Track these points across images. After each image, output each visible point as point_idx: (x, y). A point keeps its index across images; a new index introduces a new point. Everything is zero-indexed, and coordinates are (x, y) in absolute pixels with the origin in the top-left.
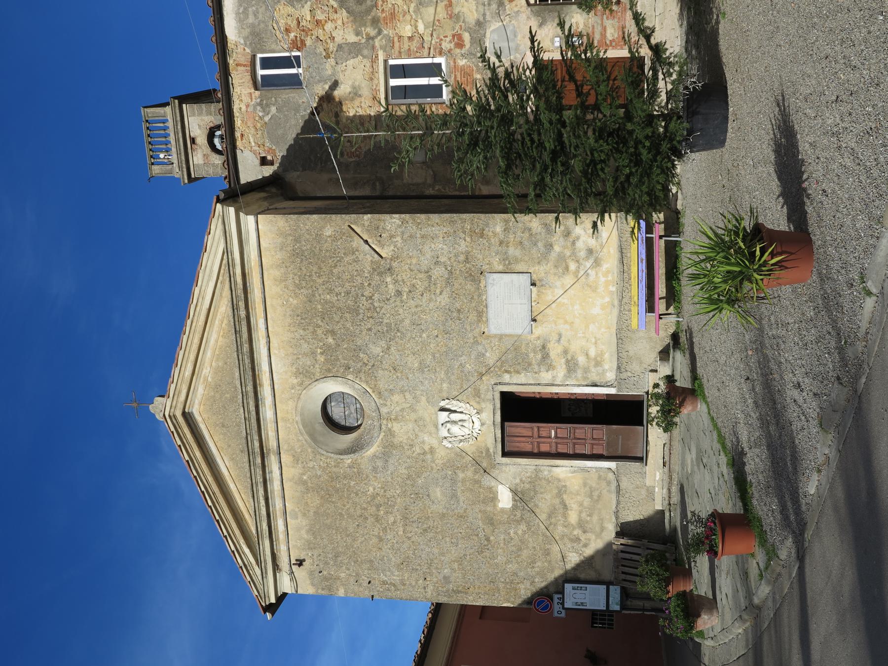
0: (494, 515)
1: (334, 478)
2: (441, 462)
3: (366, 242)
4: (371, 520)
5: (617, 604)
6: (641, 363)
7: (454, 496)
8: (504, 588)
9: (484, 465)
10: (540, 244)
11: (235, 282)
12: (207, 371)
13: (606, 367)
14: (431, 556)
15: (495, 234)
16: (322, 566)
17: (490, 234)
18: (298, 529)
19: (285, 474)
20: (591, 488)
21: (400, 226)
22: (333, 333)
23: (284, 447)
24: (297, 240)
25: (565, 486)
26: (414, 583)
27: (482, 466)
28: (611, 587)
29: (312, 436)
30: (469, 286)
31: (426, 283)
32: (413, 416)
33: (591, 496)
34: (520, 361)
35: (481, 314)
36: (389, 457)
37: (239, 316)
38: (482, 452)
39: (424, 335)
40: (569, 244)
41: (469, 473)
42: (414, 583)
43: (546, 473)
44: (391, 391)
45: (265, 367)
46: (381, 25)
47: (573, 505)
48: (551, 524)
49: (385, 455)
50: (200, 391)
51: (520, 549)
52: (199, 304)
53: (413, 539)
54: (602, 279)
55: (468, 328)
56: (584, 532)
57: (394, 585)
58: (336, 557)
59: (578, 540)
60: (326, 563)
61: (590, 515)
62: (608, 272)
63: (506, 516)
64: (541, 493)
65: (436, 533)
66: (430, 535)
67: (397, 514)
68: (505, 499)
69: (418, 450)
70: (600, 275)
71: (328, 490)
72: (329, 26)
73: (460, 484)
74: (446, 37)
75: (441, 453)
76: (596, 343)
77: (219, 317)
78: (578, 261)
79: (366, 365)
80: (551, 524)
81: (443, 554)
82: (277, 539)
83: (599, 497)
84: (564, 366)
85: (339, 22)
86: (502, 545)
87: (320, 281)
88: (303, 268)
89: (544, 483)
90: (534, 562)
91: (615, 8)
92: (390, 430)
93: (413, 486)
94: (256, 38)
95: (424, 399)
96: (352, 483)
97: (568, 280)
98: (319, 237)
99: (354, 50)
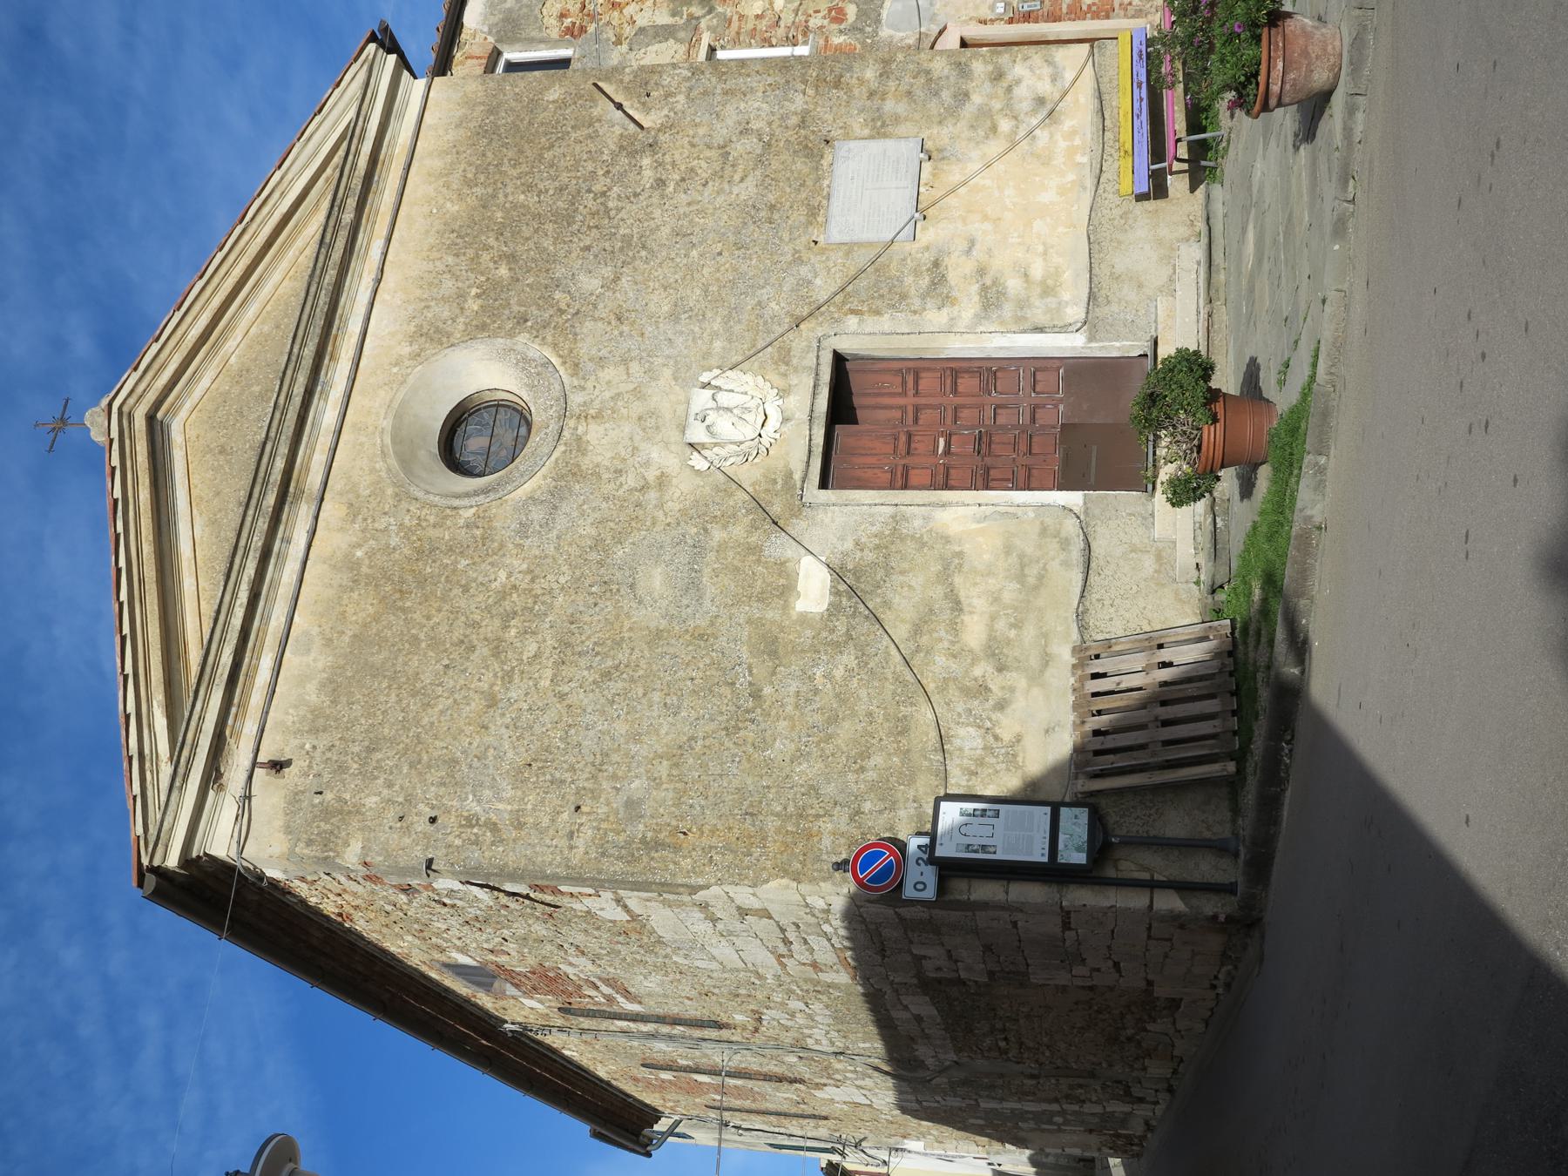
1: (424, 552)
2: (677, 507)
3: (619, 107)
4: (483, 651)
5: (1079, 849)
6: (1140, 286)
7: (693, 586)
8: (778, 831)
9: (776, 509)
10: (946, 95)
12: (234, 346)
14: (607, 743)
15: (861, 81)
16: (326, 777)
17: (854, 81)
18: (302, 680)
20: (1021, 556)
22: (512, 258)
24: (492, 111)
25: (960, 555)
26: (546, 821)
28: (1064, 811)
30: (801, 165)
31: (717, 166)
32: (637, 408)
33: (1021, 577)
34: (884, 291)
35: (815, 212)
36: (562, 499)
37: (338, 221)
38: (775, 482)
39: (694, 253)
40: (1000, 92)
41: (738, 531)
42: (546, 821)
43: (917, 523)
44: (601, 362)
45: (354, 327)
48: (918, 649)
49: (555, 497)
50: (206, 381)
51: (834, 720)
54: (1062, 145)
55: (786, 236)
57: (494, 827)
58: (370, 750)
59: (983, 689)
60: (342, 769)
61: (1016, 625)
63: (809, 633)
64: (902, 573)
65: (632, 680)
66: (616, 686)
68: (813, 590)
69: (631, 481)
70: (1058, 137)
71: (402, 579)
73: (711, 556)
74: (817, 12)
75: (682, 488)
76: (1045, 253)
77: (299, 243)
78: (1015, 118)
79: (562, 312)
80: (918, 649)
81: (636, 737)
82: (243, 706)
83: (1041, 578)
84: (976, 298)
86: (789, 708)
87: (514, 173)
88: (489, 154)
90: (865, 755)
92: (579, 439)
93: (601, 564)
95: (667, 373)
96: (464, 562)
97: (994, 147)
98: (534, 105)
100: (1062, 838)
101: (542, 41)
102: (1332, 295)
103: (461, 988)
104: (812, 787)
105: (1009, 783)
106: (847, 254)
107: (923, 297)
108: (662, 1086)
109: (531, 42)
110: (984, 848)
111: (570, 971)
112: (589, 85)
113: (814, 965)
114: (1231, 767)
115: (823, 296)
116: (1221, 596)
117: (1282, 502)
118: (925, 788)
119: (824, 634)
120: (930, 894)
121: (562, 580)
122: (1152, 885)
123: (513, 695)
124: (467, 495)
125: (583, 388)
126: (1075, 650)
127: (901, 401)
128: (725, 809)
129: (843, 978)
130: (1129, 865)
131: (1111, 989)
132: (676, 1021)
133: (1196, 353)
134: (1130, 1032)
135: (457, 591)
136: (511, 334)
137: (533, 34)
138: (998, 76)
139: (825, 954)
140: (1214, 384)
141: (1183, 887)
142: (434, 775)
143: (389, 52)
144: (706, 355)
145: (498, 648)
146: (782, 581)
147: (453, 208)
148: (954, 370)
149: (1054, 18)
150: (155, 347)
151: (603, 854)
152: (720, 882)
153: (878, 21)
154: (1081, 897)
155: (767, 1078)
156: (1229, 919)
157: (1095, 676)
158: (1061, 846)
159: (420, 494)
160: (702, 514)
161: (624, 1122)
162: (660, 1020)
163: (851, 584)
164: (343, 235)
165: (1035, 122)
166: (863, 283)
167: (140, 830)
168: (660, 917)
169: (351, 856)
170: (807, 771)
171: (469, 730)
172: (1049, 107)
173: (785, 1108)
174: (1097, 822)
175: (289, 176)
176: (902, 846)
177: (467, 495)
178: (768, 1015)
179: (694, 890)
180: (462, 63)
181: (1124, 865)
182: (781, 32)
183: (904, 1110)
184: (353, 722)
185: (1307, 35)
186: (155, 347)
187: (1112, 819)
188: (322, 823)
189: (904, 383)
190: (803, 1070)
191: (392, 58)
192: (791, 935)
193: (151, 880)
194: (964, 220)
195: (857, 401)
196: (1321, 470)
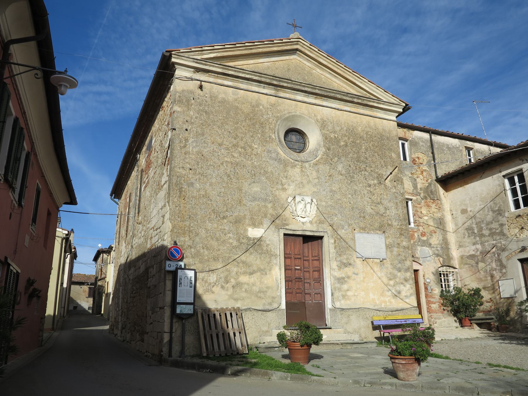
0: (243, 224)
3: (391, 173)
4: (235, 142)
5: (181, 311)
6: (346, 323)
7: (254, 199)
8: (185, 225)
9: (277, 221)
10: (400, 265)
11: (370, 101)
12: (318, 71)
13: (342, 302)
15: (402, 241)
16: (198, 101)
18: (225, 93)
19: (262, 97)
20: (266, 291)
21: (400, 192)
22: (346, 145)
24: (388, 138)
25: (266, 274)
26: (187, 161)
27: (276, 220)
28: (192, 306)
29: (287, 119)
30: (377, 225)
31: (375, 201)
32: (305, 182)
33: (260, 292)
35: (363, 229)
37: (354, 98)
38: (285, 221)
39: (350, 196)
40: (401, 281)
42: (187, 161)
43: (275, 261)
44: (318, 171)
45: (325, 103)
46: (425, 200)
47: (253, 279)
48: (238, 263)
49: (279, 160)
50: (308, 64)
51: (217, 240)
52: (359, 79)
53: (221, 167)
54: (387, 299)
55: (356, 221)
56: (233, 287)
57: (185, 147)
58: (206, 112)
60: (201, 105)
62: (391, 303)
63: (242, 232)
64: (260, 258)
65: (227, 183)
66: (226, 179)
67: (240, 159)
68: (254, 233)
69: (284, 181)
70: (389, 298)
71: (254, 119)
72: (421, 176)
73: (263, 204)
75: (283, 195)
77: (348, 88)
79: (331, 160)
80: (238, 263)
81: (211, 185)
82: (217, 77)
83: (260, 297)
84: (341, 276)
85: (423, 182)
86: (220, 227)
87: (371, 145)
89: (268, 260)
90: (208, 249)
91: (442, 308)
92: (295, 166)
93: (260, 173)
94: (414, 144)
95: (315, 190)
96: (259, 136)
97: (385, 280)
98: (390, 150)
99: (415, 186)
100: (184, 306)
101: (411, 153)
102: (337, 380)
103: (147, 142)
104: (198, 234)
105: (200, 290)
106: (352, 239)
107: (340, 261)
108: (126, 199)
109: (410, 150)
110: (181, 283)
111: (151, 171)
112: (397, 165)
113: (151, 238)
114: (205, 355)
115: (339, 232)
116: (255, 350)
117: (278, 367)
118: (198, 266)
119: (242, 236)
120: (168, 268)
121: (255, 163)
122: (171, 332)
123: (222, 150)
124: (278, 136)
125: (310, 167)
126: (238, 308)
127: (310, 256)
128: (191, 210)
129: (149, 246)
130: (177, 326)
131: (146, 322)
132: (139, 201)
133: (322, 340)
134: (137, 328)
135: (251, 134)
136: (324, 146)
137: (413, 150)
138: (406, 280)
139: (154, 240)
140: (313, 346)
141: (171, 341)
142: (199, 130)
143: (403, 109)
144: (321, 201)
145: (235, 146)
146: (257, 224)
147: (360, 129)
148: (320, 270)
149: (427, 296)
150: (317, 50)
151: (178, 177)
152: (170, 209)
153: (422, 246)
154: (167, 312)
155: (127, 227)
156: (162, 356)
157: (231, 314)
158: (182, 306)
159: (278, 123)
160: (275, 201)
161: (117, 191)
162: (140, 196)
163: (257, 243)
164: (351, 99)
165: (393, 291)
166: (344, 244)
167: (182, 51)
168: (162, 194)
169: (176, 108)
170: (203, 233)
171: (212, 139)
172: (398, 295)
173: (121, 233)
174: (189, 316)
175: (366, 84)
176: (181, 260)
177: (278, 136)
178: (140, 226)
179: (168, 202)
180: (403, 131)
181: (177, 324)
182: (417, 219)
183: (120, 266)
184: (214, 107)
185: (413, 370)
186: (317, 50)
187: (190, 320)
188: (185, 100)
189: (315, 256)
190: (129, 237)
191: (401, 110)
192: (158, 231)
193: (168, 54)
194: (363, 272)
195: (310, 243)
196: (286, 378)
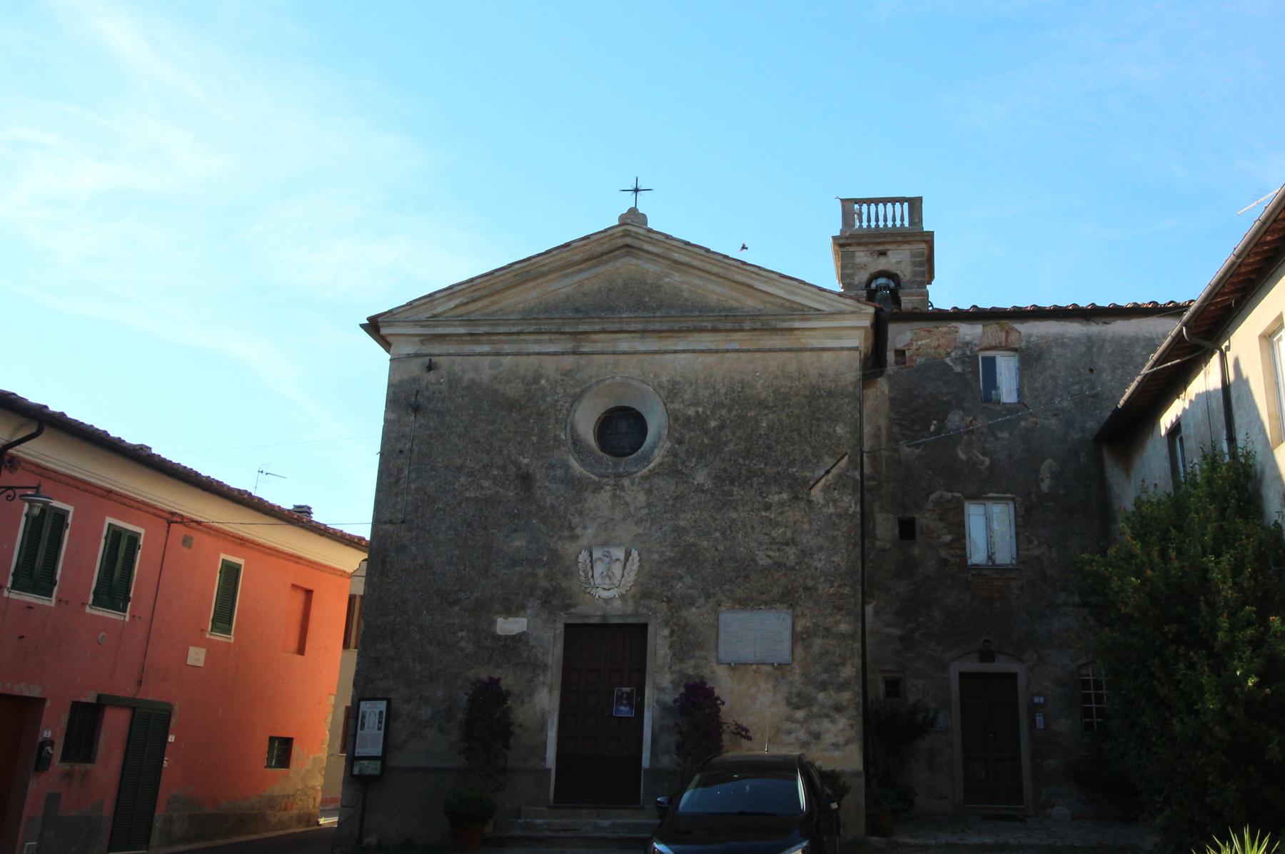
10: (825, 676)
15: (837, 623)
22: (722, 427)
23: (583, 360)
35: (744, 603)
39: (718, 534)
41: (544, 583)
55: (726, 587)
68: (509, 626)
69: (576, 520)
73: (529, 570)
75: (568, 548)
78: (805, 721)
79: (683, 463)
87: (783, 416)
92: (602, 488)
95: (640, 530)
123: (462, 479)
125: (633, 484)
135: (519, 439)
136: (669, 436)
138: (838, 708)
